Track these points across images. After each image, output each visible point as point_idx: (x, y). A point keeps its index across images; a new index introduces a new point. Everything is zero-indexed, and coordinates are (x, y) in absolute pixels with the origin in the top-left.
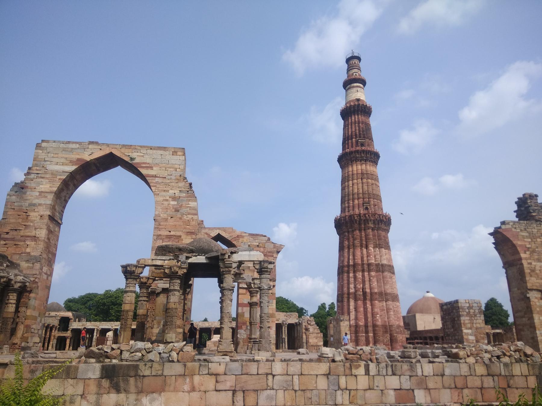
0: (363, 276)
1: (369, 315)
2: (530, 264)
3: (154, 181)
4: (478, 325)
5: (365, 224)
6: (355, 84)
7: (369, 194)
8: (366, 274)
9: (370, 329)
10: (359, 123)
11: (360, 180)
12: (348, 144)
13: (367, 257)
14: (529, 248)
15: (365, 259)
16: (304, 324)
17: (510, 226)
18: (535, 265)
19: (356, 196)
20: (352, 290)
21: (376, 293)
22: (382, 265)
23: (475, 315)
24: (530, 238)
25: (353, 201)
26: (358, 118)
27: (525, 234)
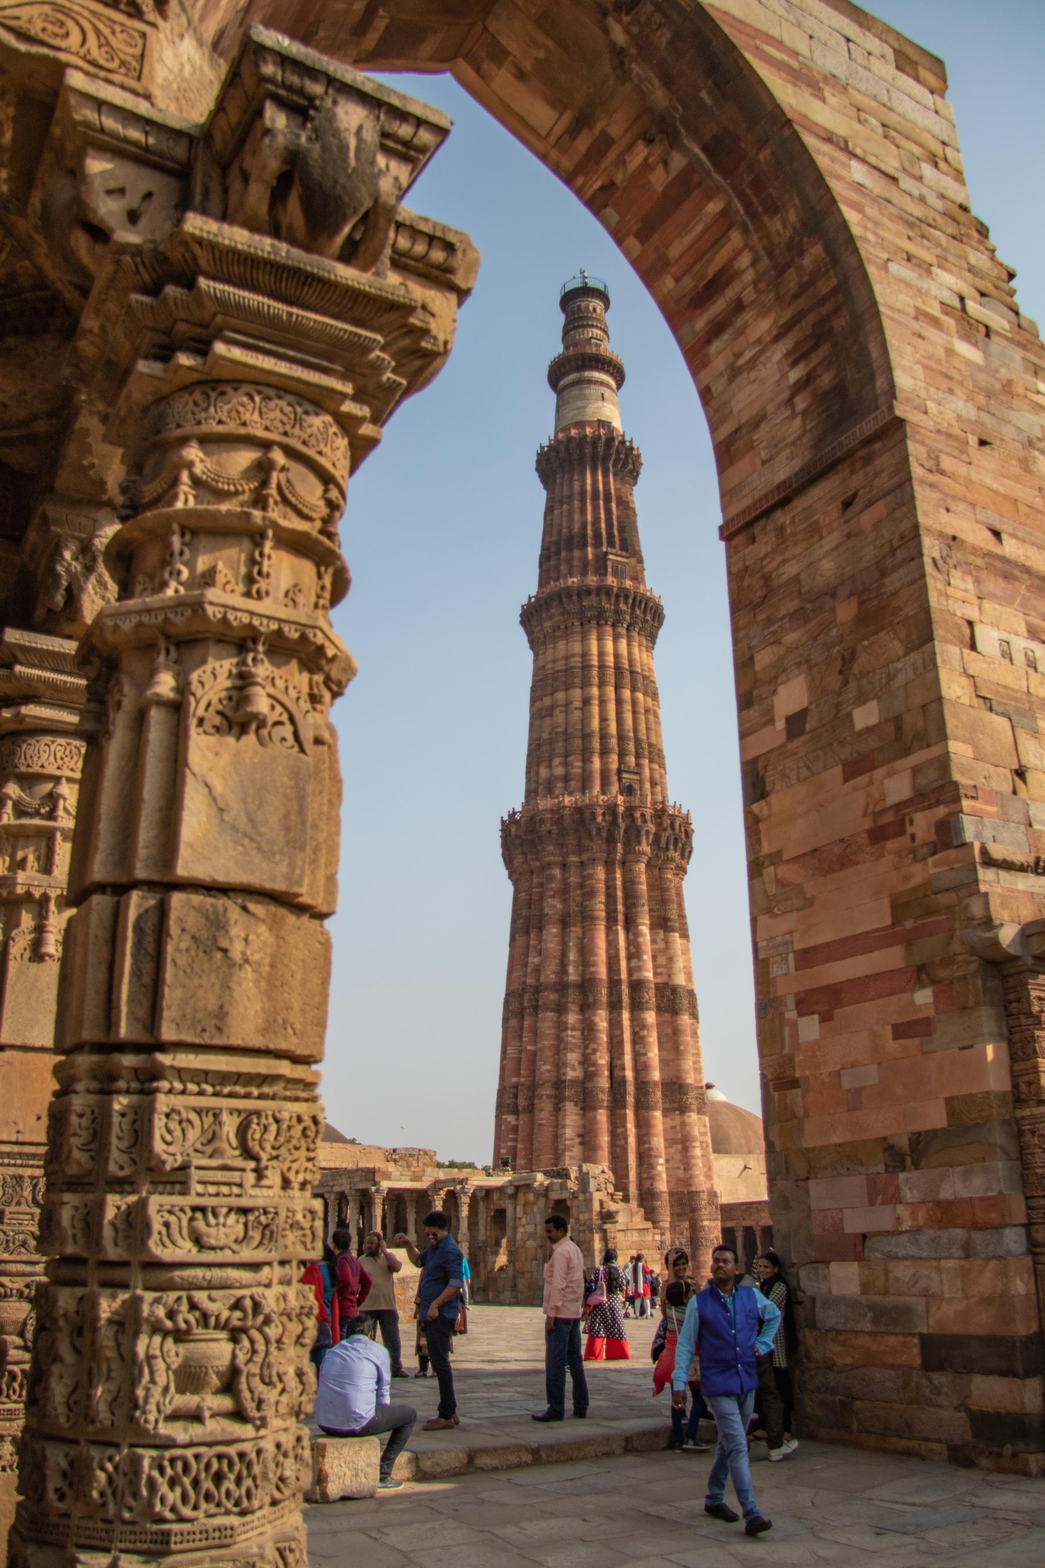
0: (615, 1024)
3: (844, 173)
5: (627, 844)
6: (597, 375)
7: (637, 741)
8: (626, 1015)
11: (610, 691)
12: (569, 561)
13: (630, 957)
15: (623, 964)
16: (597, 1196)
19: (596, 745)
20: (573, 1073)
21: (655, 1083)
22: (675, 990)
25: (586, 760)
26: (606, 484)
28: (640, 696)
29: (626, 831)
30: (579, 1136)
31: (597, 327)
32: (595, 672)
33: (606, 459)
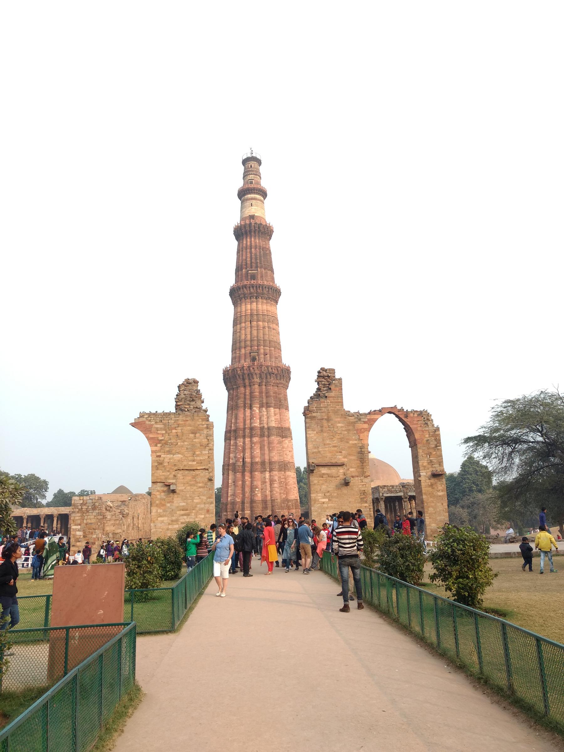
0: (244, 443)
1: (247, 490)
2: (160, 456)
4: (89, 521)
5: (249, 379)
7: (258, 340)
8: (247, 440)
9: (247, 505)
10: (251, 249)
11: (248, 324)
13: (251, 420)
14: (161, 440)
15: (248, 422)
17: (144, 419)
18: (164, 458)
19: (243, 344)
21: (257, 463)
22: (269, 428)
23: (88, 511)
24: (165, 430)
25: (240, 351)
26: (251, 241)
27: (158, 426)
28: (261, 323)
29: (248, 375)
30: (234, 482)
31: (252, 174)
32: (243, 317)
33: (250, 232)
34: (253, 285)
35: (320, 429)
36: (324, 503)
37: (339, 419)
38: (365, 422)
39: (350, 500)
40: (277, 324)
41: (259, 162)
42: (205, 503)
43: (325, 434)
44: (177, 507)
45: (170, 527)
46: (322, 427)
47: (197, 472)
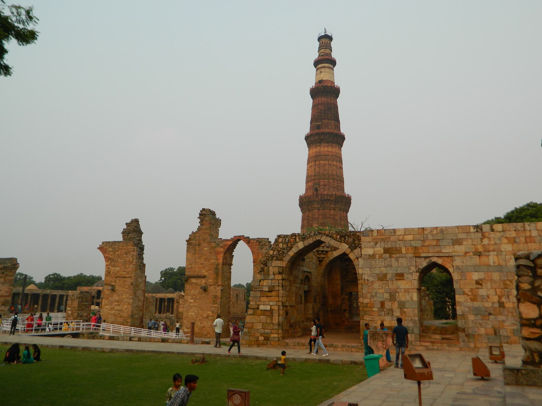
2: (109, 268)
26: (318, 101)
27: (110, 249)
34: (325, 131)
35: (194, 251)
36: (191, 302)
37: (205, 245)
38: (221, 247)
39: (207, 301)
40: (340, 161)
41: (330, 38)
42: (128, 299)
43: (197, 255)
44: (115, 300)
45: (110, 312)
46: (195, 250)
47: (127, 279)
